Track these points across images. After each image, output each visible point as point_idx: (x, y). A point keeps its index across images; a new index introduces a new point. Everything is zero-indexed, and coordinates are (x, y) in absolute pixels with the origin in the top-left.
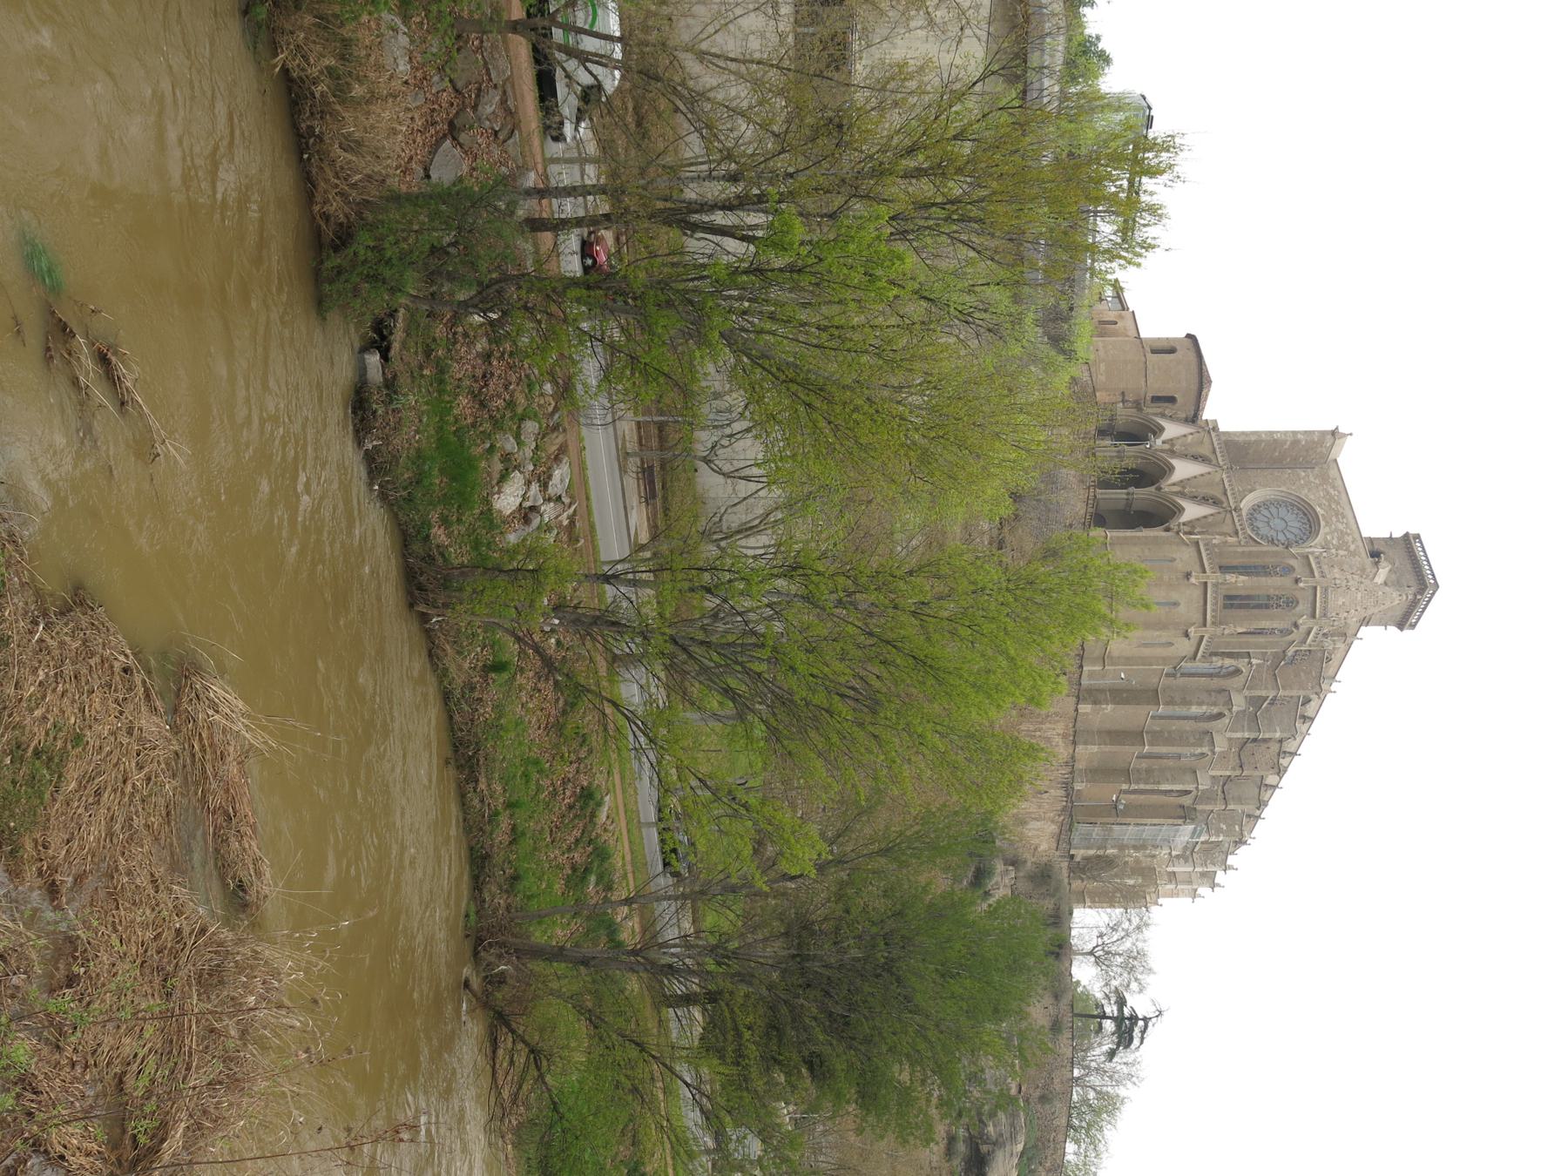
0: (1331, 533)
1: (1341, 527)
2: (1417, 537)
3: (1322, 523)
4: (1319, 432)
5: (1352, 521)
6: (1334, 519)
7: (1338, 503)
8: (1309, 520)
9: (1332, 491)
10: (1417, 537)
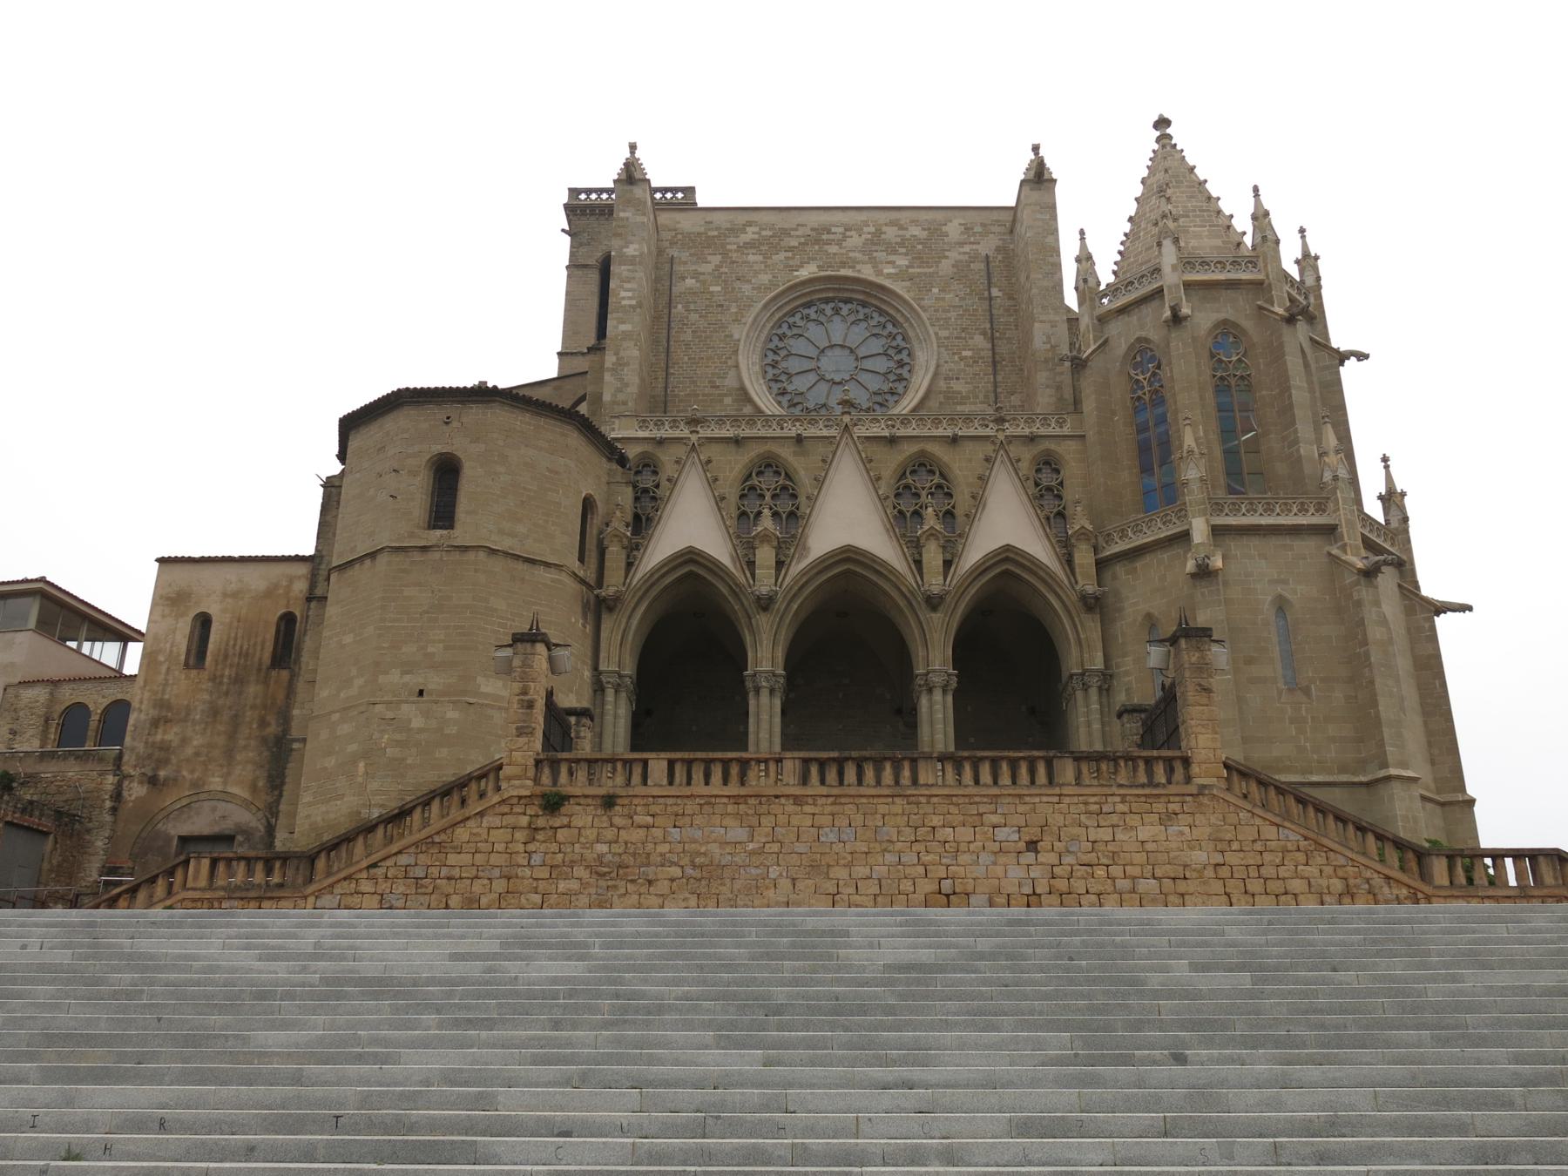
0: (874, 262)
1: (855, 240)
2: (574, 192)
5: (840, 217)
6: (833, 249)
7: (785, 232)
8: (827, 301)
10: (574, 192)
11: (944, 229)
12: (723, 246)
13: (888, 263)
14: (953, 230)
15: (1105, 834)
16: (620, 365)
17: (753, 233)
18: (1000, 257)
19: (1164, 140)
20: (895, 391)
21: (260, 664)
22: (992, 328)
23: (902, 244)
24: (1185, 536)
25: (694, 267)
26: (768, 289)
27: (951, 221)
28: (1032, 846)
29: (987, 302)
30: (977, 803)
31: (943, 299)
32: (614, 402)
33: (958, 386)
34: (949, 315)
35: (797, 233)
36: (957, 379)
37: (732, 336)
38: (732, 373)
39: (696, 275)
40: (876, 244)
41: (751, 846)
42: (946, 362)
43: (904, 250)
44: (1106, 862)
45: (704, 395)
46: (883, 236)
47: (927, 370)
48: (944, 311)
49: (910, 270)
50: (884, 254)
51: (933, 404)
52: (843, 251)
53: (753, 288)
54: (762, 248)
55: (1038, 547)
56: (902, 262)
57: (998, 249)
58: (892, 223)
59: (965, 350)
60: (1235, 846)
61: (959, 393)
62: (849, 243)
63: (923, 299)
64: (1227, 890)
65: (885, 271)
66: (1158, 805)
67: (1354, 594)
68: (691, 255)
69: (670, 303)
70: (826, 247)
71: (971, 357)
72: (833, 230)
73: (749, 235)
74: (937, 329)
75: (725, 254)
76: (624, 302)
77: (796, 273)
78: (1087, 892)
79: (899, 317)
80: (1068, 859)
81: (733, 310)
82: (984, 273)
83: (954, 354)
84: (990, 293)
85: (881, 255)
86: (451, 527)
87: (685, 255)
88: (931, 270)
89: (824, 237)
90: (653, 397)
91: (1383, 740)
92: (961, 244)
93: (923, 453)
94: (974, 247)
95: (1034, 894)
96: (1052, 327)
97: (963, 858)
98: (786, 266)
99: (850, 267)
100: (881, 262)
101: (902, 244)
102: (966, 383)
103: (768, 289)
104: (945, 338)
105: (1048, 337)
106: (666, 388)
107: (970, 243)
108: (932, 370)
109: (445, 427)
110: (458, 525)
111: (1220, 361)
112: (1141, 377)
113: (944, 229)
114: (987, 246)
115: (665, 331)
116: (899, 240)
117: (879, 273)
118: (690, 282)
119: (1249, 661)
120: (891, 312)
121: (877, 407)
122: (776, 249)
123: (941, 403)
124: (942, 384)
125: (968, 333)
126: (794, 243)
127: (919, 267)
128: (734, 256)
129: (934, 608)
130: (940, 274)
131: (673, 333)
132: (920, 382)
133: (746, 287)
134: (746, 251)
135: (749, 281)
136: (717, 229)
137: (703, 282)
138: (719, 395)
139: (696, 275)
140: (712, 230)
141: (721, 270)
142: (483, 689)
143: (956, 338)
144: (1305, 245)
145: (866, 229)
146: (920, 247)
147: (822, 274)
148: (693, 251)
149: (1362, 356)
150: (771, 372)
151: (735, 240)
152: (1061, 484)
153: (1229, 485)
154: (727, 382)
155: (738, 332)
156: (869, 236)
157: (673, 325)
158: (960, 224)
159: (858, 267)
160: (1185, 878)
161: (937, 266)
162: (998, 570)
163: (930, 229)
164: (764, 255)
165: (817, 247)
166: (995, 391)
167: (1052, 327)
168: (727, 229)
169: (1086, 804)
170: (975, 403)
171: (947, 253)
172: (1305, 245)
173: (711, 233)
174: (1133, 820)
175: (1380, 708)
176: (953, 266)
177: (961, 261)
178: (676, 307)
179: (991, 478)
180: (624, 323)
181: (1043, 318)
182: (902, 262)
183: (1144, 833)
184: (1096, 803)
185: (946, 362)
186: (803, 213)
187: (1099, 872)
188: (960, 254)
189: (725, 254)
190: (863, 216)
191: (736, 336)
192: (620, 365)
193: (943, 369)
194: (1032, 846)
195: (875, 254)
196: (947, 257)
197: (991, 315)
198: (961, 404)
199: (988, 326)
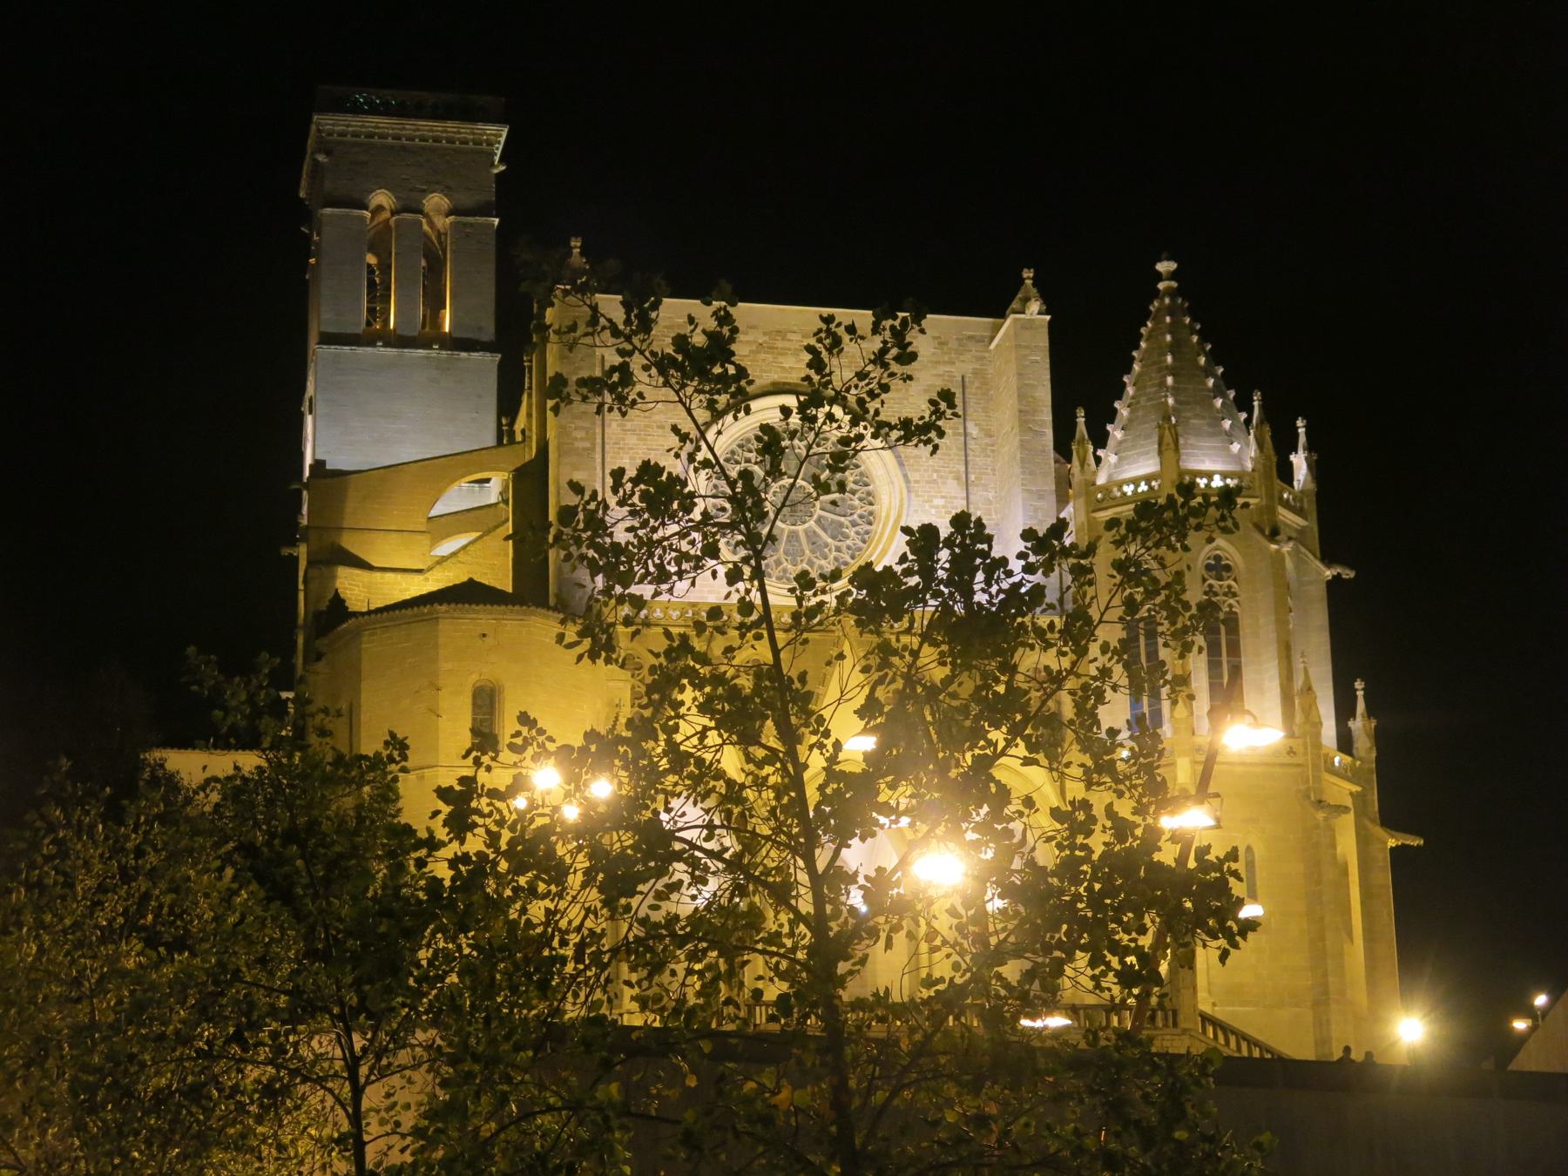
59: (936, 497)
70: (781, 359)
89: (780, 344)
107: (944, 362)
125: (941, 477)
143: (928, 482)
157: (607, 447)
165: (770, 357)
178: (610, 425)
185: (916, 511)
199: (963, 469)
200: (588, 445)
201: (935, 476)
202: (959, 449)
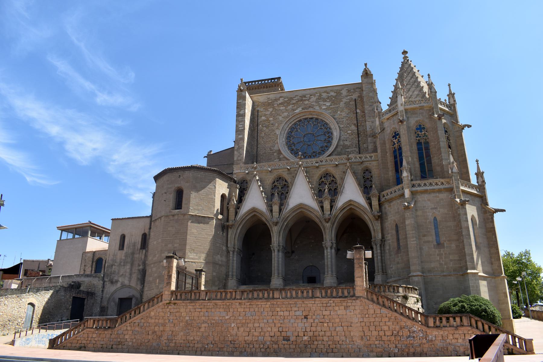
0: (320, 106)
1: (313, 99)
3: (311, 109)
4: (237, 100)
5: (308, 92)
6: (307, 102)
9: (279, 102)
11: (341, 92)
12: (273, 105)
13: (324, 105)
14: (344, 92)
15: (327, 313)
16: (239, 148)
17: (282, 100)
18: (359, 99)
19: (405, 58)
20: (327, 146)
21: (138, 248)
22: (357, 123)
23: (328, 98)
24: (403, 195)
25: (265, 113)
26: (287, 117)
27: (343, 89)
28: (306, 317)
29: (356, 114)
30: (291, 304)
31: (341, 115)
32: (238, 160)
33: (347, 143)
34: (343, 120)
35: (296, 98)
36: (346, 140)
37: (276, 133)
38: (276, 146)
39: (265, 115)
40: (320, 99)
41: (227, 317)
42: (343, 135)
43: (328, 100)
44: (328, 321)
45: (268, 153)
46: (322, 96)
47: (337, 139)
48: (342, 119)
49: (331, 107)
50: (322, 102)
51: (339, 149)
52: (310, 103)
53: (282, 118)
54: (285, 104)
55: (361, 200)
56: (328, 104)
57: (359, 97)
58: (325, 92)
60: (367, 316)
61: (347, 145)
62: (311, 100)
63: (335, 115)
64: (364, 330)
65: (323, 108)
66: (345, 303)
67: (458, 211)
68: (264, 109)
69: (258, 125)
70: (304, 102)
71: (351, 133)
72: (307, 96)
73: (281, 100)
74: (339, 125)
75: (274, 108)
76: (240, 129)
77: (295, 111)
78: (321, 331)
79: (327, 122)
80: (316, 321)
81: (276, 125)
82: (354, 105)
83: (345, 132)
84: (356, 111)
85: (321, 103)
86: (181, 209)
87: (262, 110)
88: (337, 106)
89: (304, 99)
90: (253, 155)
91: (466, 260)
92: (347, 96)
93: (327, 170)
94: (351, 97)
95: (306, 331)
96: (372, 123)
97: (286, 321)
98: (292, 109)
99: (312, 108)
100: (322, 105)
101: (328, 98)
102: (349, 141)
103: (287, 117)
104: (342, 128)
105: (371, 126)
106: (257, 151)
107: (350, 96)
108: (338, 138)
109: (179, 179)
110: (183, 208)
111: (418, 134)
112: (394, 141)
113: (341, 92)
114: (355, 96)
115: (256, 134)
116: (327, 97)
117: (321, 108)
118: (263, 118)
119: (424, 236)
120: (326, 120)
121: (322, 152)
122: (289, 104)
123: (341, 149)
124: (341, 143)
126: (294, 102)
127: (334, 105)
128: (277, 108)
129: (327, 222)
130: (340, 106)
131: (259, 134)
132: (335, 142)
133: (280, 118)
134: (280, 106)
135: (281, 115)
136: (271, 100)
137: (267, 117)
138: (273, 153)
139: (265, 115)
140: (269, 100)
141: (273, 113)
142: (190, 257)
144: (450, 90)
145: (317, 95)
146: (334, 99)
147: (303, 111)
148: (264, 107)
149: (469, 126)
150: (289, 143)
151: (276, 103)
152: (372, 177)
153: (421, 175)
154: (275, 148)
155: (278, 132)
156: (318, 97)
157: (258, 132)
158: (346, 90)
159: (314, 107)
160: (351, 326)
161: (339, 104)
162: (348, 208)
163: (336, 92)
164: (286, 107)
165: (301, 102)
166: (359, 144)
167: (372, 123)
168: (275, 100)
169: (322, 303)
170: (352, 148)
171: (342, 100)
172: (450, 90)
173: (269, 102)
174: (337, 308)
175: (466, 250)
176: (344, 104)
177: (347, 102)
179: (345, 179)
180: (240, 135)
181: (369, 120)
182: (328, 104)
183: (339, 312)
184: (325, 303)
185: (343, 135)
186: (297, 92)
187: (325, 325)
188: (346, 99)
189: (274, 108)
190: (316, 91)
191: (277, 134)
192: (239, 148)
193: (342, 138)
194: (306, 317)
195: (320, 103)
196: (342, 101)
197: (357, 118)
198: (349, 148)
199: (356, 122)
200: (243, 128)
201: (348, 126)
202: (355, 117)
